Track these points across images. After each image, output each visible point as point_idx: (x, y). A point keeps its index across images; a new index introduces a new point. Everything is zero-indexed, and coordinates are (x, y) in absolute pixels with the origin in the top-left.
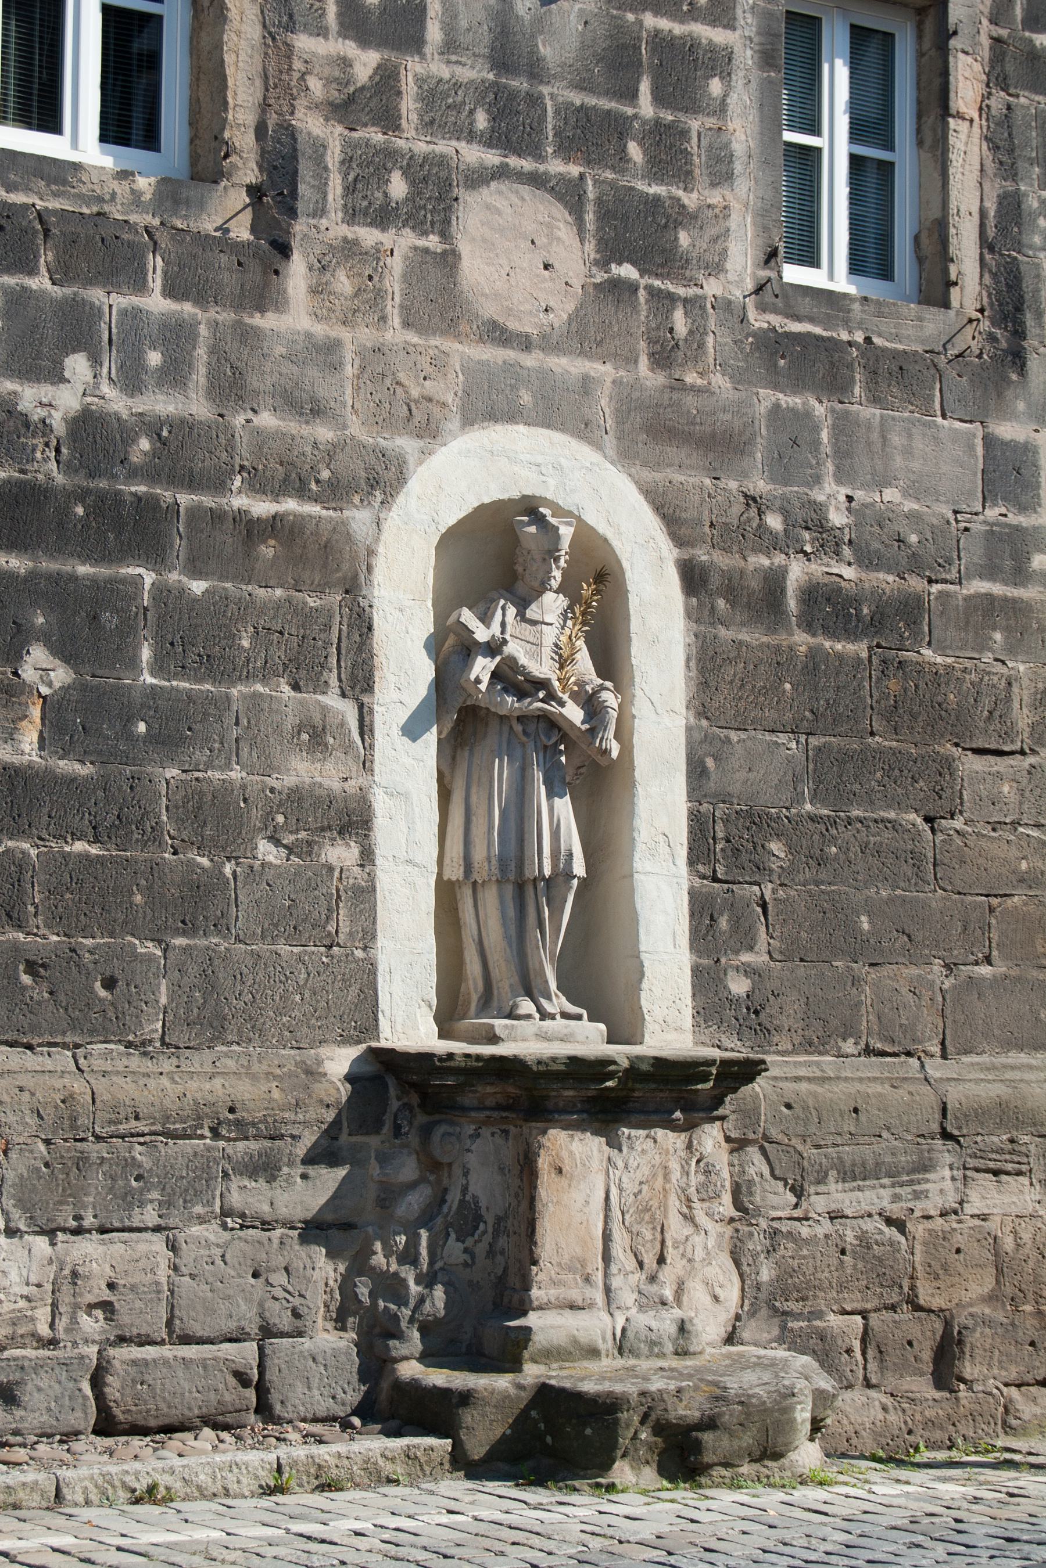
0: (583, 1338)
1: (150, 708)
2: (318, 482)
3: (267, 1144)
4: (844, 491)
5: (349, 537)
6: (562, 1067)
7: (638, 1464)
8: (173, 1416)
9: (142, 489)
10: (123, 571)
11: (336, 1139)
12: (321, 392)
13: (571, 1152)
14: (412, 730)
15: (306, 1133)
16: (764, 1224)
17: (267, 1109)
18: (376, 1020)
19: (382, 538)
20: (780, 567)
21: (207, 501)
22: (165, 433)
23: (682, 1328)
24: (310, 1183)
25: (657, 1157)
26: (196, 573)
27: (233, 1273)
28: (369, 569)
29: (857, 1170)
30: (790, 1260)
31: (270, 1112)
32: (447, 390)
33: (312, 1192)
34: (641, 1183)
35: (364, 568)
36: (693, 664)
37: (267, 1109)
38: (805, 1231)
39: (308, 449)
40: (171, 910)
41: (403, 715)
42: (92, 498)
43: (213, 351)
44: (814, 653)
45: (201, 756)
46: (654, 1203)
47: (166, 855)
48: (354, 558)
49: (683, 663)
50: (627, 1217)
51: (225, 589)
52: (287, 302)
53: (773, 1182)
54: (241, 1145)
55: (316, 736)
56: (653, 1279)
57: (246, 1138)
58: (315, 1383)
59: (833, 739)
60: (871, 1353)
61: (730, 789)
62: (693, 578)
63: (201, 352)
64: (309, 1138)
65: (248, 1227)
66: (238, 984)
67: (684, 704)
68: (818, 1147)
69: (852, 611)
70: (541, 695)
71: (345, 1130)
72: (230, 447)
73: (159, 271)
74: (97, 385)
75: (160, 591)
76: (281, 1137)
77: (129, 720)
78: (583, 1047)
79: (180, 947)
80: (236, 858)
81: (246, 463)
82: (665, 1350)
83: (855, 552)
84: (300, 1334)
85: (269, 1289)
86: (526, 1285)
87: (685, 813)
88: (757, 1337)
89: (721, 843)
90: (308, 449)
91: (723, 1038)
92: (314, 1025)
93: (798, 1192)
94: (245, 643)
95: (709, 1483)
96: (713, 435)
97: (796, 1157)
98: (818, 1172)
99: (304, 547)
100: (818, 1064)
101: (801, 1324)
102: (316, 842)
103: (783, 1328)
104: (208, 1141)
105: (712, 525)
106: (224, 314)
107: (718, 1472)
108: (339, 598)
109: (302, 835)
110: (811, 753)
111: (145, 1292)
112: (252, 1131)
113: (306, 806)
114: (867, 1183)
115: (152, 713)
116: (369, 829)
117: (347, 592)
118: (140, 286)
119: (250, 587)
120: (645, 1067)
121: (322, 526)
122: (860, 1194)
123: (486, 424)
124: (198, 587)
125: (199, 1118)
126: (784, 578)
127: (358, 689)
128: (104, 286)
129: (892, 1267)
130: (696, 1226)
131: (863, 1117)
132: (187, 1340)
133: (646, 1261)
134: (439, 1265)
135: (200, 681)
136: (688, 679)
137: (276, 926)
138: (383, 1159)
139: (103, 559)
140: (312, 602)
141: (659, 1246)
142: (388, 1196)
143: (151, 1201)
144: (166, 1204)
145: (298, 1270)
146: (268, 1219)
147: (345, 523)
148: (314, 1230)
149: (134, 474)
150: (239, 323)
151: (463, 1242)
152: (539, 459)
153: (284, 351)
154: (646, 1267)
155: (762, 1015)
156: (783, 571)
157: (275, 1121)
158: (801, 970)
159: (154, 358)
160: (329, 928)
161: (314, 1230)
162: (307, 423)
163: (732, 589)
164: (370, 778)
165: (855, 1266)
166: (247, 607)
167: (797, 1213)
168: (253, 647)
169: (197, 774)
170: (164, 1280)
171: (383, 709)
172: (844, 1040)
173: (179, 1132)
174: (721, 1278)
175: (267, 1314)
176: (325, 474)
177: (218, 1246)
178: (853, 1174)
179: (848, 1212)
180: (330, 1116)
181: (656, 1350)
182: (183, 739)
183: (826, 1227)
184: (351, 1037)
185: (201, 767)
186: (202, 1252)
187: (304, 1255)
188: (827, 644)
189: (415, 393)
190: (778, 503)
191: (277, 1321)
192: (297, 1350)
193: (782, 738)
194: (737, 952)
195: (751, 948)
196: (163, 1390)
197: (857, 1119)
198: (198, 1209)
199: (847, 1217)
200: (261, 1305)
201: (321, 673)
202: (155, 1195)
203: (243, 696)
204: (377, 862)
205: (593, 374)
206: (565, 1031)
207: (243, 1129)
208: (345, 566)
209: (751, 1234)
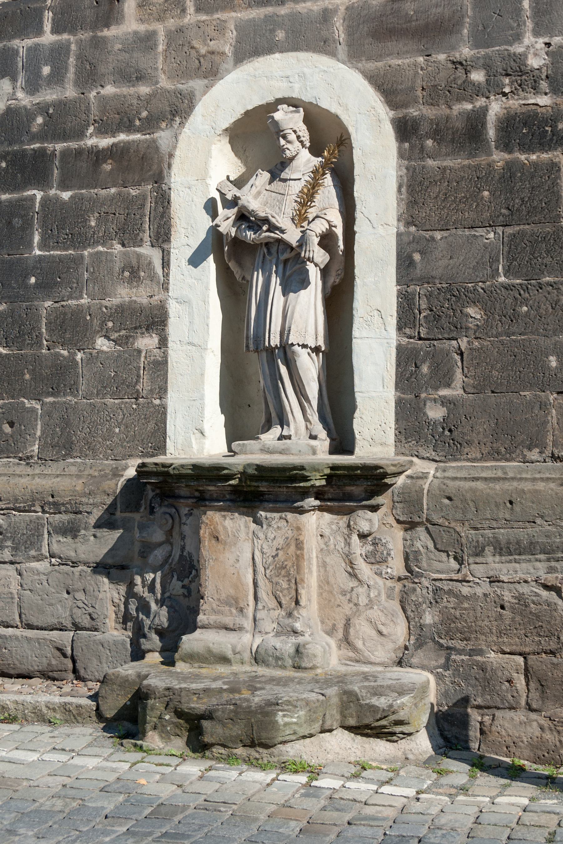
0: (216, 649)
1: (37, 268)
2: (140, 120)
3: (72, 516)
4: (540, 42)
5: (157, 149)
6: (190, 472)
7: (166, 736)
8: (23, 669)
9: (38, 145)
10: (25, 194)
11: (114, 514)
12: (142, 66)
13: (225, 528)
14: (196, 260)
15: (95, 510)
16: (426, 583)
17: (71, 496)
18: (165, 442)
19: (178, 145)
20: (481, 107)
21: (73, 145)
22: (51, 111)
23: (298, 651)
24: (98, 541)
25: (290, 532)
26: (64, 186)
27: (53, 591)
28: (170, 166)
29: (512, 548)
30: (452, 611)
31: (74, 498)
33: (98, 544)
34: (277, 549)
35: (166, 166)
36: (404, 190)
37: (71, 496)
38: (465, 590)
39: (135, 102)
40: (45, 382)
41: (189, 253)
42: (10, 156)
43: (79, 57)
44: (510, 166)
45: (65, 292)
46: (289, 564)
47: (44, 351)
48: (161, 161)
49: (395, 189)
50: (268, 572)
51: (82, 194)
52: (123, 17)
53: (437, 553)
54: (57, 516)
55: (134, 272)
56: (290, 615)
57: (60, 513)
58: (104, 661)
59: (527, 227)
60: (532, 685)
61: (434, 273)
62: (405, 130)
63: (72, 60)
64: (97, 513)
65: (63, 564)
66: (81, 423)
67: (396, 218)
68: (476, 529)
69: (548, 129)
70: (265, 228)
71: (119, 509)
72: (88, 109)
73: (50, 20)
74: (14, 93)
75: (45, 201)
76: (80, 512)
77: (26, 277)
78: (296, 457)
79: (50, 403)
80: (83, 349)
81: (96, 118)
82: (286, 664)
83: (550, 85)
84: (96, 630)
85: (75, 601)
86: (196, 611)
87: (395, 293)
88: (426, 662)
89: (426, 312)
90: (135, 102)
91: (421, 450)
92: (125, 447)
93: (459, 560)
94: (93, 224)
95: (210, 756)
96: (427, 25)
97: (455, 536)
98: (476, 547)
99: (129, 161)
100: (503, 468)
101: (463, 657)
102: (131, 336)
103: (448, 659)
104: (40, 514)
105: (423, 89)
106: (86, 34)
107: (217, 750)
108: (150, 187)
109: (123, 332)
110: (506, 239)
111: (4, 598)
112: (63, 509)
113: (125, 314)
114: (523, 557)
115: (39, 271)
116: (165, 325)
117: (156, 183)
118: (39, 32)
119: (96, 190)
120: (251, 471)
121: (140, 146)
122: (517, 565)
124: (66, 195)
125: (34, 500)
126: (485, 115)
127: (160, 240)
128: (20, 37)
129: (549, 622)
130: (359, 581)
131: (517, 508)
132: (30, 627)
133: (283, 602)
134: (167, 594)
135: (66, 249)
136: (399, 201)
137: (105, 387)
138: (142, 527)
139: (15, 189)
140: (134, 192)
141: (294, 593)
142: (147, 549)
143: (7, 547)
144: (15, 549)
145: (90, 592)
146: (75, 561)
147: (154, 141)
148: (102, 568)
149: (34, 138)
150: (94, 37)
151: (182, 581)
152: (289, 73)
153: (120, 46)
154: (284, 606)
155: (455, 433)
156: (485, 110)
157: (76, 503)
158: (492, 399)
159: (46, 70)
160: (138, 387)
161: (102, 568)
163: (439, 131)
164: (166, 294)
165: (513, 619)
166: (95, 202)
167: (459, 576)
168: (97, 225)
169: (63, 303)
170: (15, 592)
171: (177, 251)
172: (530, 449)
173: (22, 509)
174: (383, 619)
175: (74, 616)
176: (144, 114)
177: (44, 574)
178: (508, 550)
179: (503, 578)
180: (109, 501)
181: (280, 663)
182: (56, 284)
183: (485, 588)
184: (148, 453)
185: (65, 299)
186: (36, 577)
187: (93, 583)
188: (523, 157)
189: (203, 51)
190: (482, 61)
191: (80, 621)
192: (92, 639)
193: (480, 232)
194: (436, 388)
195: (448, 385)
196: (16, 654)
197: (512, 509)
198: (33, 553)
199: (503, 582)
200: (71, 610)
201: (138, 234)
202: (9, 543)
203: (90, 255)
204: (169, 345)
205: (330, 7)
206: (283, 447)
207: (57, 508)
208: (155, 167)
209: (414, 590)
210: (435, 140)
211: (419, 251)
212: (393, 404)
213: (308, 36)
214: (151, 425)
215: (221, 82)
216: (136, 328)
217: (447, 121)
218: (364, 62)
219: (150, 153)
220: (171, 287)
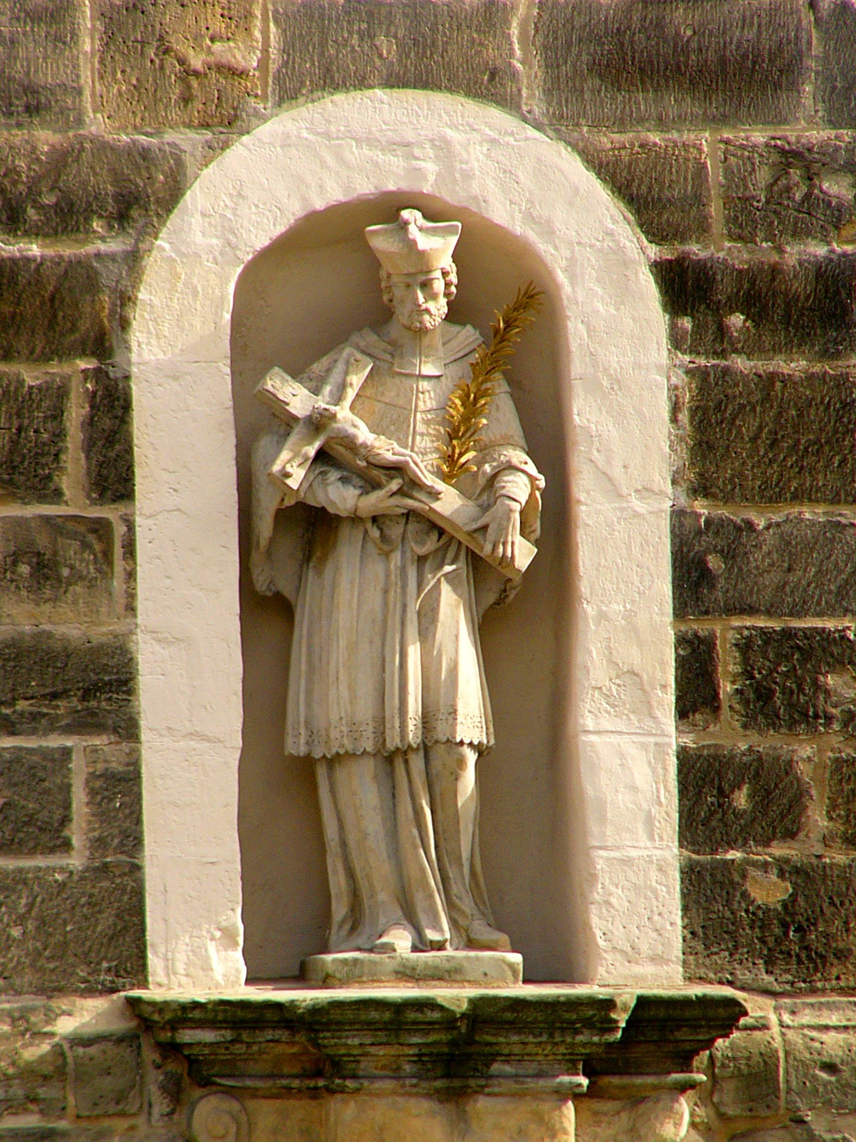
28: (125, 324)
32: (253, 48)
36: (684, 417)
39: (22, 164)
49: (666, 415)
62: (683, 287)
116: (131, 692)
162: (19, 125)
189: (197, 61)
194: (767, 843)
204: (143, 737)
214: (106, 921)
216: (54, 696)
217: (773, 279)
220: (141, 605)
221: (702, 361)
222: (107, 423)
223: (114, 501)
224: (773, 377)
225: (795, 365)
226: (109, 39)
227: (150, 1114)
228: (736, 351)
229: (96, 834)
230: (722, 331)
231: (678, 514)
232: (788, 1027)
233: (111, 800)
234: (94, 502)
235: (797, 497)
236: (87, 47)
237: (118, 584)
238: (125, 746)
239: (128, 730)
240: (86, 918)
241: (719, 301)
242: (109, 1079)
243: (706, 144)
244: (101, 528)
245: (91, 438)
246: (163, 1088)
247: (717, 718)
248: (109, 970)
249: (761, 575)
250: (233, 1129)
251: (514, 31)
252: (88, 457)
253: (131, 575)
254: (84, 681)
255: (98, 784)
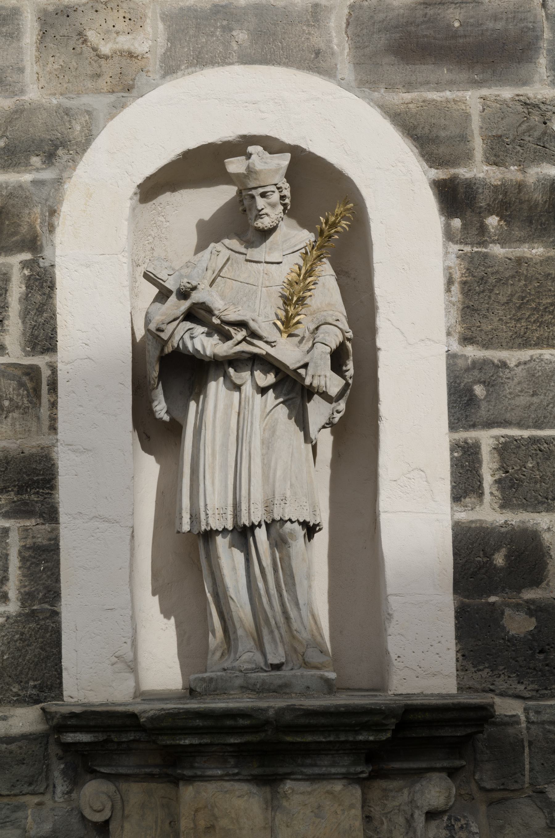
28: (52, 229)
32: (149, 40)
36: (456, 288)
62: (454, 198)
123: (190, 70)
189: (105, 49)
194: (519, 590)
208: (24, 229)
210: (502, 217)
211: (484, 383)
212: (452, 614)
213: (277, 42)
215: (140, 100)
217: (520, 192)
218: (383, 90)
219: (13, 206)
220: (61, 426)
221: (468, 249)
222: (38, 298)
223: (42, 353)
224: (519, 261)
225: (536, 251)
226: (43, 34)
227: (54, 792)
228: (494, 242)
229: (27, 589)
230: (483, 229)
231: (451, 357)
232: (533, 723)
233: (38, 565)
234: (27, 354)
235: (538, 344)
236: (28, 41)
237: (44, 411)
238: (47, 527)
239: (51, 515)
240: (18, 649)
241: (481, 207)
242: (24, 767)
243: (472, 100)
244: (32, 372)
245: (26, 308)
246: (64, 773)
247: (481, 502)
248: (35, 687)
249: (513, 398)
250: (109, 806)
251: (332, 24)
252: (24, 322)
253: (54, 405)
254: (19, 480)
255: (27, 554)
